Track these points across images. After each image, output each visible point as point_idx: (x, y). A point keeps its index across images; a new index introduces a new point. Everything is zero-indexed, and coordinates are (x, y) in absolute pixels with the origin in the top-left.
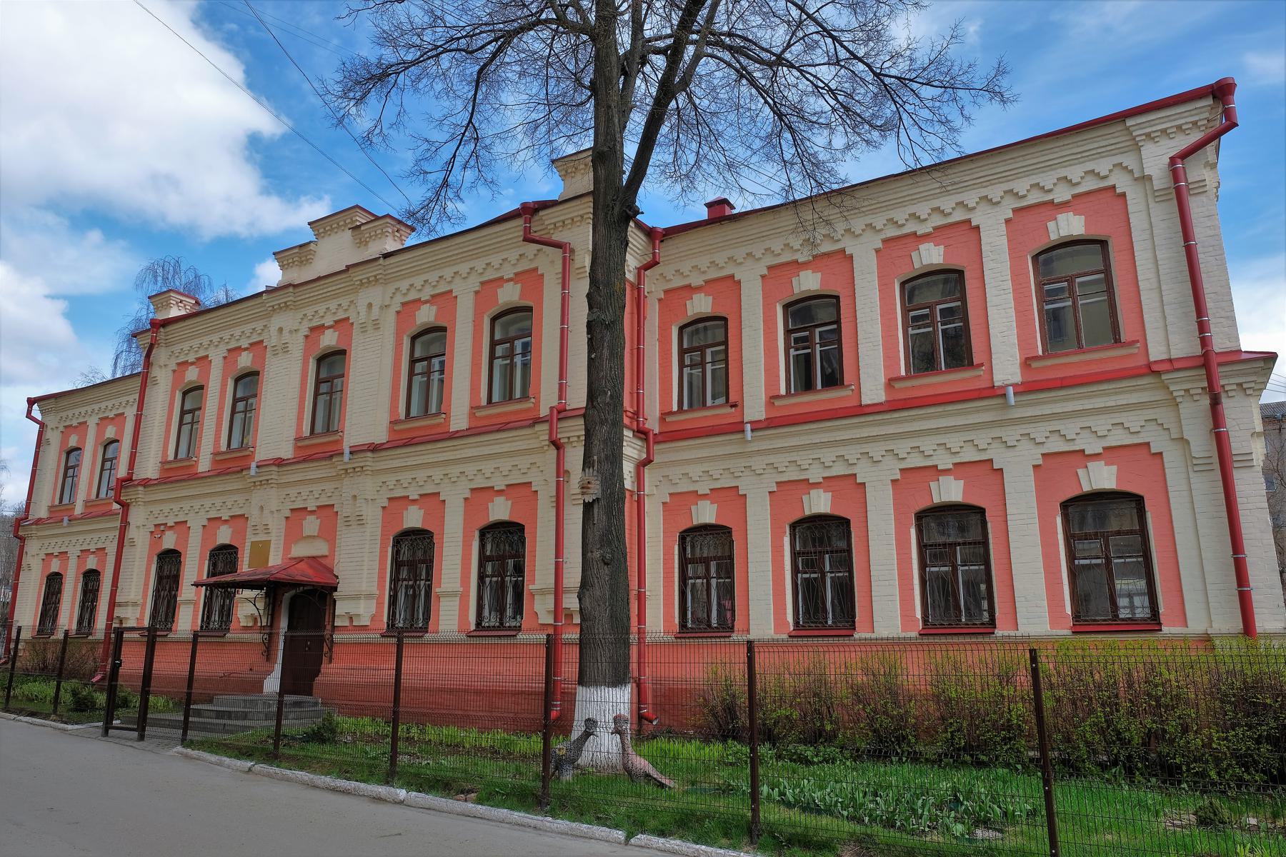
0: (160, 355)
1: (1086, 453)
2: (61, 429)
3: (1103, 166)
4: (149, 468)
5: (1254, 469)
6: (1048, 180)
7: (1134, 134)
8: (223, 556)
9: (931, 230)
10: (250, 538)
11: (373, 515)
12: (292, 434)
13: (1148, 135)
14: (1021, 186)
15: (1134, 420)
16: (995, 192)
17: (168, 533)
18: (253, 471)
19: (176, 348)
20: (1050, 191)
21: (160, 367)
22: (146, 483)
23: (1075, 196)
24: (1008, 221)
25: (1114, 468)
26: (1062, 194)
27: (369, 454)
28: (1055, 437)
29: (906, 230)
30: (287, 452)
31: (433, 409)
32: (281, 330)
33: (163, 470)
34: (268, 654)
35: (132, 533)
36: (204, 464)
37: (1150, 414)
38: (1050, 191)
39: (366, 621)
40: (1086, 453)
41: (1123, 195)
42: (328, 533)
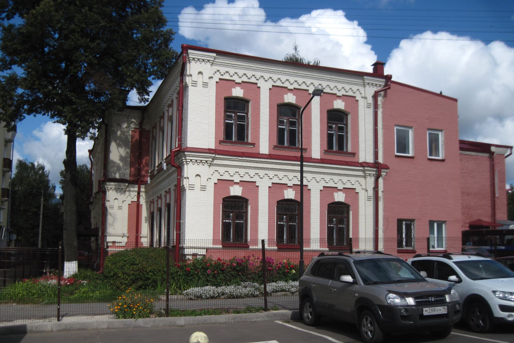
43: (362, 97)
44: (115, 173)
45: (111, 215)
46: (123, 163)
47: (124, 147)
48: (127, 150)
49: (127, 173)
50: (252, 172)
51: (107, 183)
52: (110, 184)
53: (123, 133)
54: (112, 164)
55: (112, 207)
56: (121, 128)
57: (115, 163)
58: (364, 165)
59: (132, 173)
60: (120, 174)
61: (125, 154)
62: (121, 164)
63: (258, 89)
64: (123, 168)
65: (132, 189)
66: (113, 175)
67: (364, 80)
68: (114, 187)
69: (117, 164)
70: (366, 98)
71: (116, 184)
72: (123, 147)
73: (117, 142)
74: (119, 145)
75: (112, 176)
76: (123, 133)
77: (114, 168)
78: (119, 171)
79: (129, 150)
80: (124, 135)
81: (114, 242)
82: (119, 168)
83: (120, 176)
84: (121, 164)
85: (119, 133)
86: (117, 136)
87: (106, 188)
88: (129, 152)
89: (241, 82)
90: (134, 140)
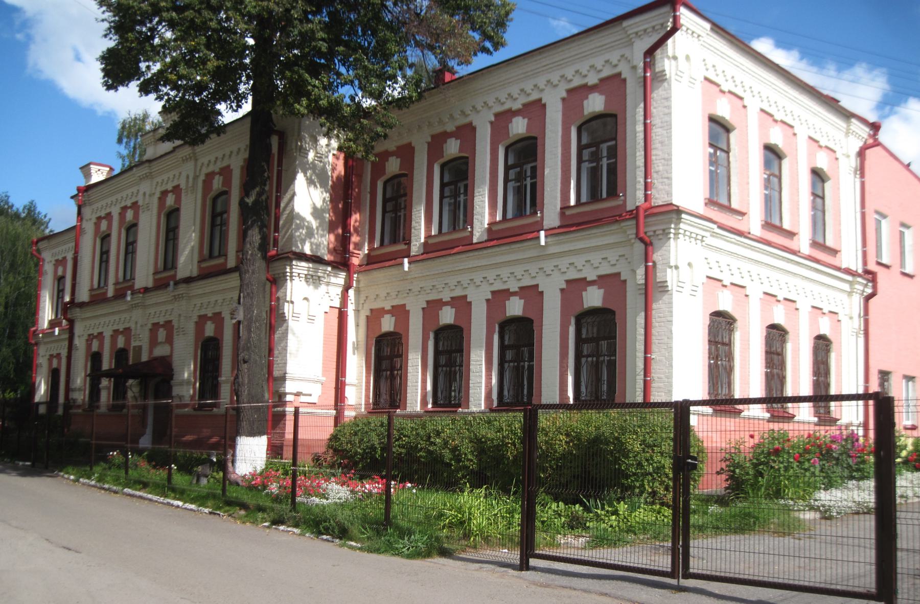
0: (87, 211)
1: (588, 279)
2: (53, 262)
3: (614, 57)
4: (83, 295)
5: (669, 293)
6: (584, 67)
7: (629, 32)
8: (121, 355)
9: (520, 107)
10: (134, 344)
11: (191, 327)
12: (151, 271)
13: (636, 33)
14: (569, 72)
15: (612, 255)
16: (555, 77)
17: (94, 341)
18: (129, 298)
19: (95, 206)
20: (585, 76)
21: (87, 220)
22: (82, 305)
23: (602, 80)
24: (563, 99)
25: (602, 291)
26: (592, 80)
27: (184, 285)
28: (572, 268)
29: (506, 107)
30: (150, 284)
31: (216, 253)
32: (144, 194)
33: (91, 296)
34: (144, 425)
35: (77, 341)
36: (110, 293)
37: (621, 251)
38: (585, 76)
39: (187, 400)
40: (588, 279)
41: (625, 80)
42: (170, 340)
43: (843, 155)
44: (303, 242)
45: (294, 334)
46: (318, 221)
47: (321, 187)
48: (324, 193)
49: (323, 242)
50: (746, 266)
51: (294, 263)
52: (299, 264)
53: (319, 157)
54: (298, 222)
55: (296, 317)
56: (317, 145)
57: (303, 219)
58: (848, 271)
59: (331, 246)
60: (311, 244)
61: (321, 203)
62: (314, 224)
63: (743, 110)
64: (317, 234)
65: (333, 280)
66: (300, 245)
67: (848, 126)
68: (306, 272)
69: (308, 222)
70: (848, 156)
71: (311, 265)
72: (318, 186)
73: (308, 174)
74: (310, 182)
75: (298, 247)
76: (319, 157)
77: (301, 230)
78: (310, 238)
79: (328, 195)
80: (321, 162)
81: (298, 394)
82: (310, 234)
83: (312, 250)
84: (314, 224)
85: (311, 155)
86: (308, 161)
87: (288, 274)
88: (328, 199)
89: (727, 90)
90: (335, 175)
